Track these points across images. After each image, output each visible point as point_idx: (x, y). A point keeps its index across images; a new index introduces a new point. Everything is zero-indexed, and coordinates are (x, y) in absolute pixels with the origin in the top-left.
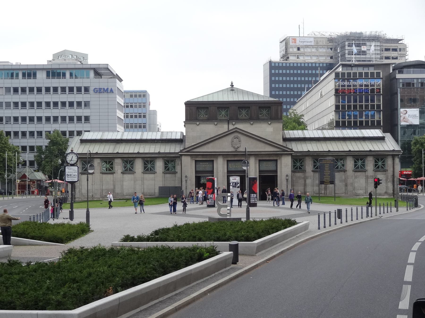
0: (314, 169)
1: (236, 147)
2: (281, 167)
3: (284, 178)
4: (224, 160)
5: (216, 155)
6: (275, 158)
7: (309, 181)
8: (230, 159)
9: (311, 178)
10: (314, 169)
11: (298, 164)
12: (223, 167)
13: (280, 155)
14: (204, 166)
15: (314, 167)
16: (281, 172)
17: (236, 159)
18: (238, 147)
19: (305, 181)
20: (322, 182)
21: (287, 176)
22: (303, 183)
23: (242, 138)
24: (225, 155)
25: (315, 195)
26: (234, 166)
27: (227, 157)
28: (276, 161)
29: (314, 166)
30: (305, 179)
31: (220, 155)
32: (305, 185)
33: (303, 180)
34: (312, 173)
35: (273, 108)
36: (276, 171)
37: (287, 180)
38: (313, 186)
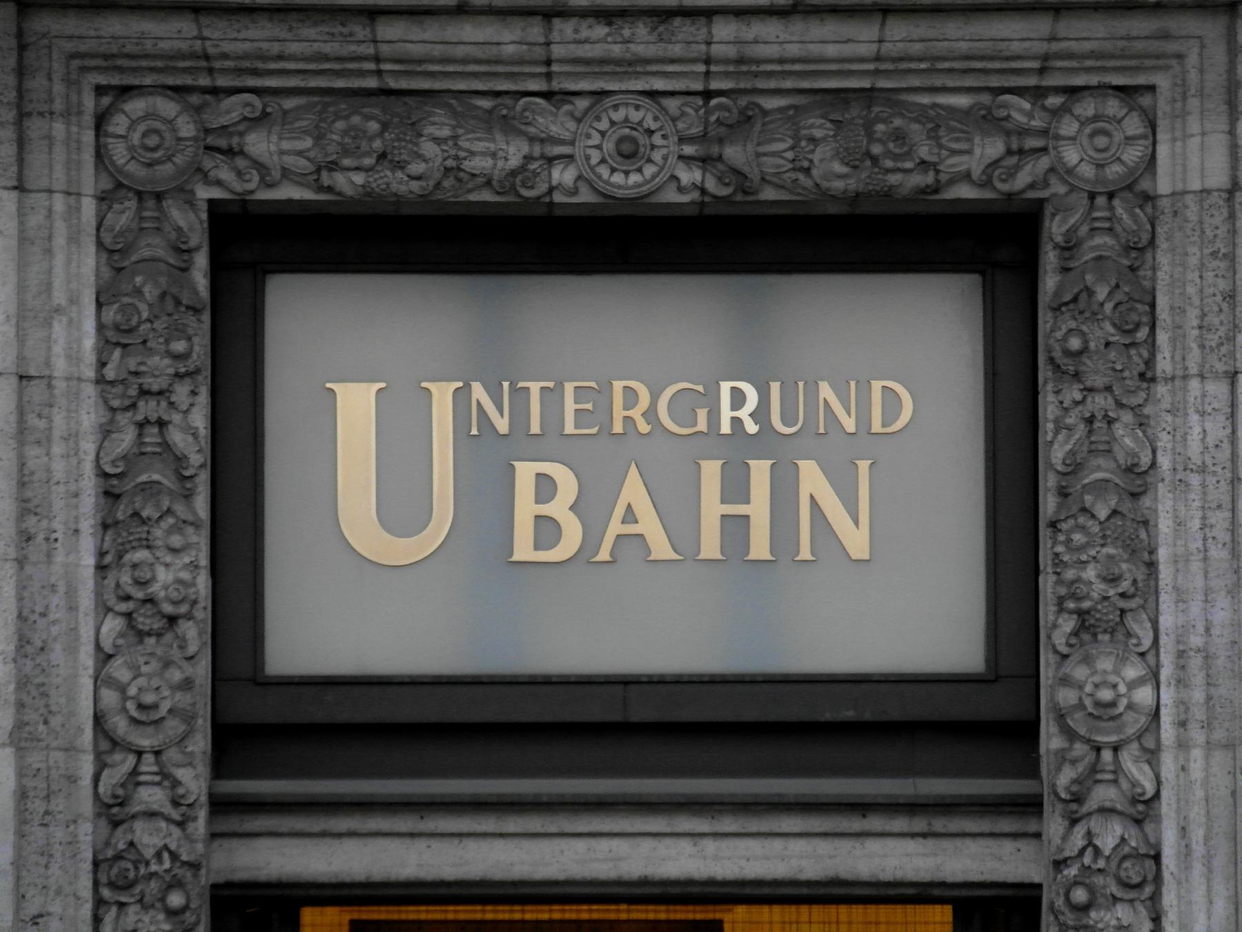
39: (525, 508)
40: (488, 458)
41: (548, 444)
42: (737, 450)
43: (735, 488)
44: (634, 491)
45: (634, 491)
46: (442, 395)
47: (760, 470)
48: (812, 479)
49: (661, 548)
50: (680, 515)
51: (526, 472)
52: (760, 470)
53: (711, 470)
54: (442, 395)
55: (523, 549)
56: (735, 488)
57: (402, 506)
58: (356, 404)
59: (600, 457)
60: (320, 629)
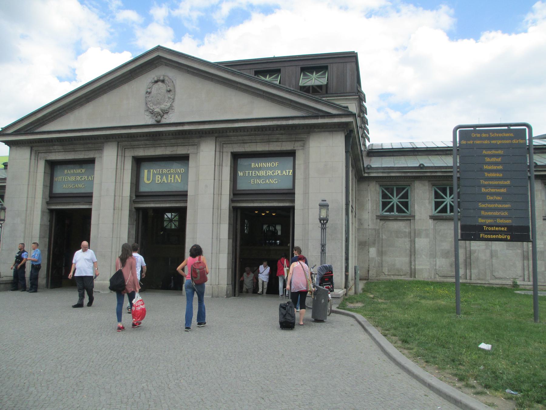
0: (435, 213)
1: (157, 110)
2: (306, 179)
3: (314, 214)
4: (121, 155)
5: (96, 141)
6: (287, 147)
7: (422, 243)
8: (141, 153)
9: (427, 236)
10: (435, 213)
11: (395, 200)
12: (118, 180)
13: (300, 132)
14: (73, 178)
15: (436, 209)
16: (306, 193)
17: (159, 152)
18: (165, 112)
19: (413, 242)
20: (471, 232)
21: (324, 206)
22: (408, 247)
23: (181, 82)
24: (124, 139)
25: (438, 279)
26: (158, 178)
27: (133, 147)
28: (292, 154)
29: (437, 204)
30: (412, 236)
31: (108, 139)
32: (412, 253)
33: (407, 240)
34: (431, 221)
35: (334, 68)
36: (290, 194)
37: (324, 222)
38: (433, 255)
39: (157, 179)
40: (154, 175)
41: (159, 174)
42: (171, 174)
43: (171, 177)
44: (164, 177)
45: (164, 177)
46: (152, 171)
47: (173, 176)
48: (177, 176)
49: (166, 182)
50: (167, 179)
51: (157, 176)
52: (173, 176)
53: (169, 176)
54: (152, 171)
55: (157, 182)
56: (171, 177)
57: (148, 179)
58: (146, 171)
59: (162, 175)
60: (143, 189)
